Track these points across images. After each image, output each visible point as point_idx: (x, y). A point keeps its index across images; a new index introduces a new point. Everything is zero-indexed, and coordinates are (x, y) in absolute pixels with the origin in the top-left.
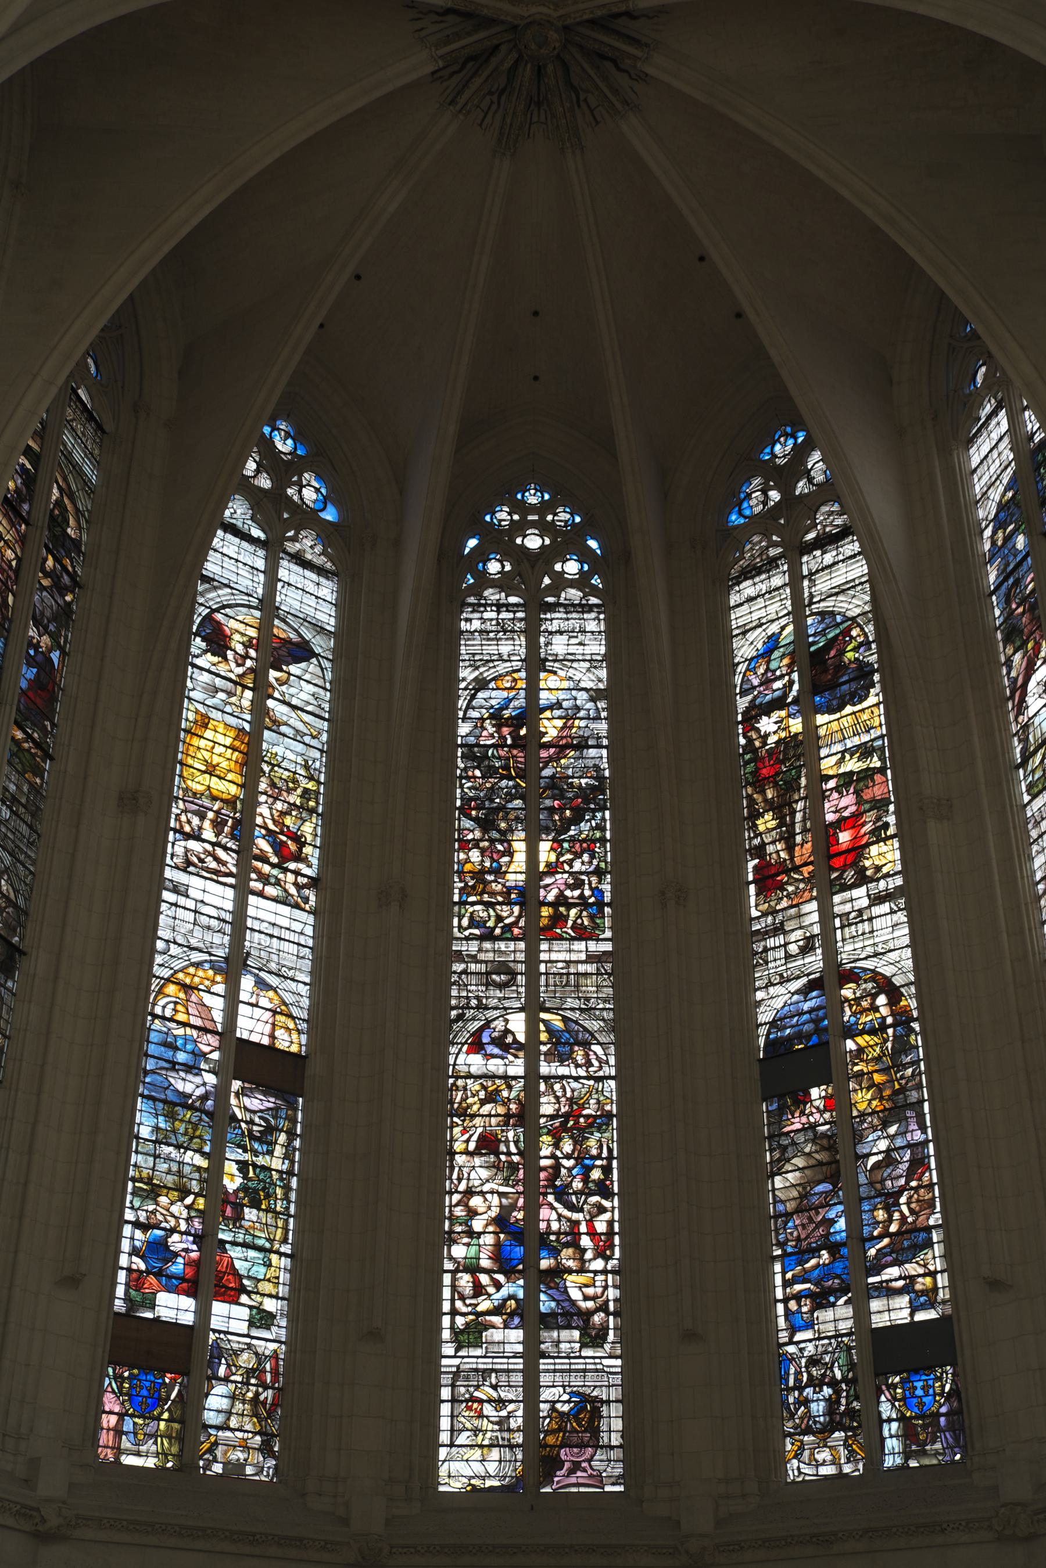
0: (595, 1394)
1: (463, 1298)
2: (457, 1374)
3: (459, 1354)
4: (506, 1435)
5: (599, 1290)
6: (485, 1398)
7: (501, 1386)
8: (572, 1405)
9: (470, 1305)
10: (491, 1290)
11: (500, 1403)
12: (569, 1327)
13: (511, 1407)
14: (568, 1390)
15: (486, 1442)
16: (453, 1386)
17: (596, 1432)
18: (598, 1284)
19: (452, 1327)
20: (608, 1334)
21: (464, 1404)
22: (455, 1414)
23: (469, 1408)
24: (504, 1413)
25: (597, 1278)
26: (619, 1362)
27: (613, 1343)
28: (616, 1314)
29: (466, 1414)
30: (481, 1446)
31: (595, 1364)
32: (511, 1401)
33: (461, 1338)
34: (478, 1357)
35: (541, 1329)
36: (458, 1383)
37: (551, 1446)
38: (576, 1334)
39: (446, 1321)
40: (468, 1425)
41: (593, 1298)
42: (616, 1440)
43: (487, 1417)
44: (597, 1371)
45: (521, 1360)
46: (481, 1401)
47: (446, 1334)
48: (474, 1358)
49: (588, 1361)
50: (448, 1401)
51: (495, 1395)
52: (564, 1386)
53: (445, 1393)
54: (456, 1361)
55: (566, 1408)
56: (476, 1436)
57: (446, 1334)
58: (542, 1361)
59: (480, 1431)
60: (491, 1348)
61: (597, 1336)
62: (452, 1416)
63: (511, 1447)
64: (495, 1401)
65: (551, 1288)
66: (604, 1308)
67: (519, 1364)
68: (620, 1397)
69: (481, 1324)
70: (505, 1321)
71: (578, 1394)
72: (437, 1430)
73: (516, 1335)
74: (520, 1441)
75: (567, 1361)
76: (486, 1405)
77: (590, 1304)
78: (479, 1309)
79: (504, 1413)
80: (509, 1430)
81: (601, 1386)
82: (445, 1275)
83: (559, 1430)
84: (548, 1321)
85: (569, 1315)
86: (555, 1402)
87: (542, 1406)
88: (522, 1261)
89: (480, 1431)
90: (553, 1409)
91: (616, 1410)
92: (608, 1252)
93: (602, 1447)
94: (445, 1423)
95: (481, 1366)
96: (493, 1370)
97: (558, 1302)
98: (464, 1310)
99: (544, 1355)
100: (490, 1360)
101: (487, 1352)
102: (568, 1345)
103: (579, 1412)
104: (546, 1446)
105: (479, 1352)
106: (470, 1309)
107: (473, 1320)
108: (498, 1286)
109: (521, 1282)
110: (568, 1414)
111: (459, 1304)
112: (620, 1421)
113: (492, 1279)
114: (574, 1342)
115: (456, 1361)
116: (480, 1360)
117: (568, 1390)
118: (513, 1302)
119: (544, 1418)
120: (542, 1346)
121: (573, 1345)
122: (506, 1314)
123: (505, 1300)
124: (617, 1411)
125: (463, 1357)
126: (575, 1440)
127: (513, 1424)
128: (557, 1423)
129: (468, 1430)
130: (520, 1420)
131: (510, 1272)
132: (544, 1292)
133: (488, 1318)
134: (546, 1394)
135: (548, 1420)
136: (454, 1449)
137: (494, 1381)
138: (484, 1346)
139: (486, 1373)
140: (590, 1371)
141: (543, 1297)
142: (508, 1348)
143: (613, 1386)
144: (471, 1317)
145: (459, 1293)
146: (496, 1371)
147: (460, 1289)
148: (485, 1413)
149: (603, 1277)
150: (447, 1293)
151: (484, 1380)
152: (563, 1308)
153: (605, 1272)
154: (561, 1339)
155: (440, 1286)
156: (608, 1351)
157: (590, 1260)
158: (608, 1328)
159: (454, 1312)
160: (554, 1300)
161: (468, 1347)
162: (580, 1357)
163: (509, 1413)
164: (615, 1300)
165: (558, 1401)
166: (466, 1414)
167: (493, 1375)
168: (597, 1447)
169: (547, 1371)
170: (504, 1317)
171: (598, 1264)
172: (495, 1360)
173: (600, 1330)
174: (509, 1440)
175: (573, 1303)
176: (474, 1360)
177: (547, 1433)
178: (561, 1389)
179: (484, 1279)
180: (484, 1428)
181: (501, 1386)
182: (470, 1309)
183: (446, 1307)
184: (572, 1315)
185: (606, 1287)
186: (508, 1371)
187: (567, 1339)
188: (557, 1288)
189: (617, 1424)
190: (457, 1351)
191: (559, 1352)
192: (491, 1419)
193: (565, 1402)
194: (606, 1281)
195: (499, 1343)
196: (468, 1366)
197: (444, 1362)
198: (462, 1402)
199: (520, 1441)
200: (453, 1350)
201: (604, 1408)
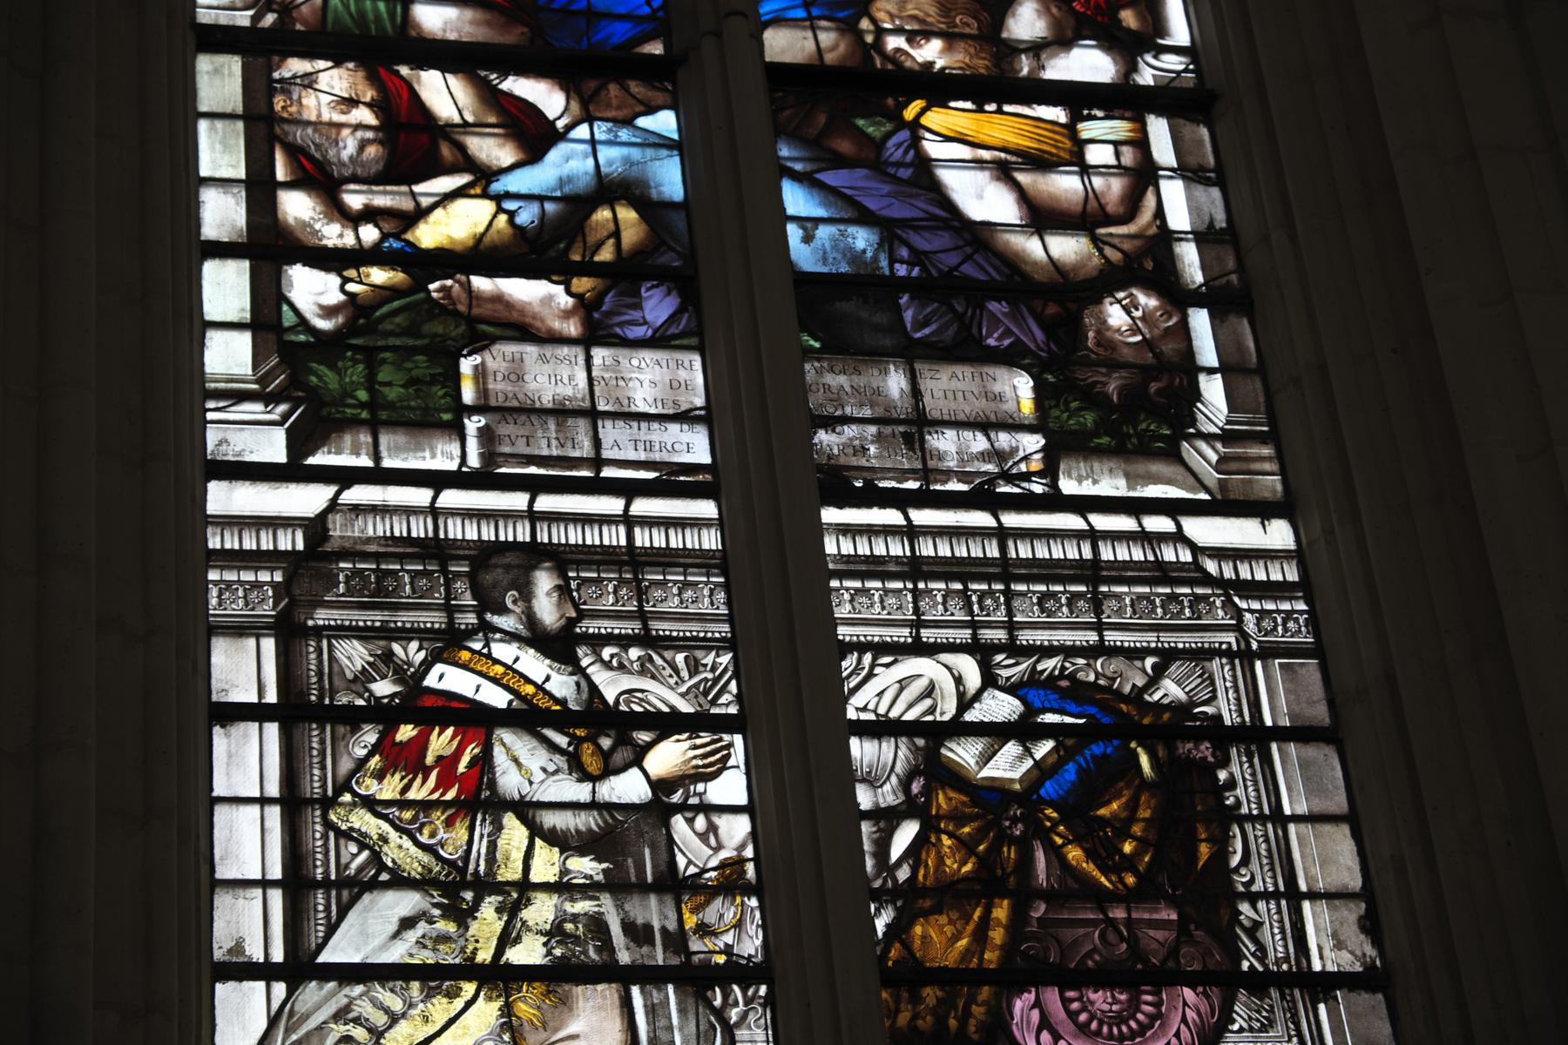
0: (1171, 690)
1: (321, 180)
2: (314, 559)
3: (319, 459)
4: (654, 912)
5: (1112, 188)
6: (497, 698)
7: (596, 642)
8: (1044, 748)
9: (370, 215)
10: (494, 150)
11: (600, 733)
12: (966, 349)
13: (668, 756)
14: (1011, 670)
15: (529, 952)
16: (290, 632)
17: (1211, 900)
18: (1099, 155)
19: (267, 317)
20: (1197, 395)
21: (370, 736)
22: (313, 784)
23: (409, 760)
24: (629, 787)
25: (1088, 129)
26: (1279, 535)
27: (1227, 437)
28: (1216, 299)
29: (389, 789)
30: (499, 977)
31: (1144, 537)
32: (667, 724)
33: (325, 377)
34: (437, 481)
35: (808, 353)
36: (322, 617)
37: (947, 978)
38: (1020, 389)
39: (225, 289)
40: (402, 852)
41: (1086, 219)
42: (1330, 941)
43: (525, 809)
44: (1161, 573)
45: (707, 509)
46: (474, 719)
47: (228, 355)
48: (411, 484)
49: (1101, 522)
50: (255, 713)
51: (562, 685)
52: (982, 652)
53: (241, 669)
54: (308, 499)
55: (1008, 765)
56: (463, 916)
57: (228, 355)
58: (830, 515)
59: (486, 885)
60: (514, 439)
61: (1134, 401)
62: (293, 802)
63: (697, 979)
64: (562, 718)
65: (839, 162)
66: (1150, 263)
67: (696, 521)
68: (1320, 714)
69: (443, 310)
70: (585, 306)
71: (1071, 692)
72: (201, 883)
73: (654, 378)
74: (751, 945)
75: (982, 519)
76: (509, 740)
77: (1067, 247)
78: (428, 235)
79: (629, 787)
80: (672, 884)
81: (1201, 655)
82: (205, 64)
83: (986, 885)
84: (846, 315)
85: (955, 294)
86: (934, 733)
87: (862, 750)
88: (657, 26)
89: (486, 885)
90: (933, 770)
91: (1300, 782)
92: (1129, 18)
93: (1259, 984)
94: (246, 843)
95: (455, 530)
96: (535, 553)
97: (890, 231)
98: (334, 235)
99: (841, 486)
100: (518, 501)
101: (489, 457)
102: (979, 443)
103: (1094, 787)
104: (911, 975)
105: (442, 457)
106: (369, 234)
107: (389, 292)
108: (535, 136)
109: (665, 122)
110: (1029, 794)
111: (297, 206)
112: (1342, 843)
113: (492, 98)
114: (1015, 426)
115: (308, 499)
116: (451, 498)
117: (1011, 670)
118: (627, 215)
119: (887, 819)
120: (823, 437)
121: (1004, 439)
122: (588, 268)
123: (577, 205)
124: (1313, 786)
125: (345, 477)
126: (1088, 941)
127: (691, 848)
128: (966, 847)
129: (400, 881)
130: (736, 829)
131: (600, 79)
132: (806, 179)
133: (481, 283)
134: (877, 691)
135: (906, 834)
136: (311, 992)
137: (547, 610)
138: (473, 424)
139: (497, 569)
140: (1123, 572)
141: (796, 200)
142: (618, 441)
143: (1268, 652)
144: (379, 276)
145: (296, 153)
146: (562, 559)
147: (299, 135)
148: (510, 781)
149: (1118, 128)
150: (219, 153)
151: (489, 603)
152: (918, 257)
153: (1120, 99)
154: (935, 404)
155: (183, 115)
156: (1212, 476)
157: (1037, 49)
158: (1190, 368)
159: (269, 248)
160: (864, 217)
161: (375, 427)
162: (1055, 502)
163: (661, 786)
164: (1204, 237)
165: (958, 728)
166: (389, 789)
167: (544, 582)
168: (1226, 981)
169: (873, 568)
170: (583, 284)
171: (1088, 64)
172: (545, 503)
173: (1147, 373)
174: (676, 940)
175: (979, 235)
176: (420, 496)
177: (913, 901)
178: (969, 667)
179: (443, 95)
180: (510, 872)
181: (596, 642)
182: (369, 234)
183: (221, 214)
184: (978, 293)
185: (1144, 175)
186: (632, 561)
187: (966, 409)
188: (872, 158)
189: (1328, 858)
190: (300, 442)
191: (926, 474)
192: (550, 819)
193: (997, 733)
194: (1141, 143)
195: (561, 412)
196: (376, 528)
197: (223, 498)
198: (353, 719)
199: (751, 945)
200: (279, 436)
201: (1237, 768)
